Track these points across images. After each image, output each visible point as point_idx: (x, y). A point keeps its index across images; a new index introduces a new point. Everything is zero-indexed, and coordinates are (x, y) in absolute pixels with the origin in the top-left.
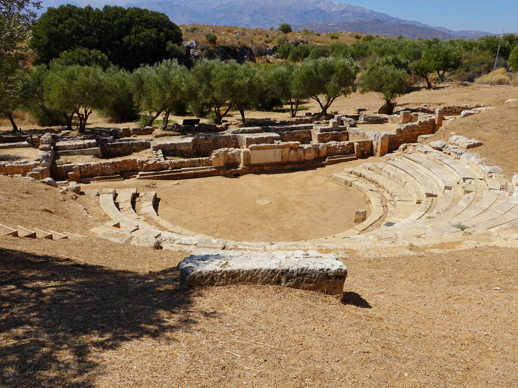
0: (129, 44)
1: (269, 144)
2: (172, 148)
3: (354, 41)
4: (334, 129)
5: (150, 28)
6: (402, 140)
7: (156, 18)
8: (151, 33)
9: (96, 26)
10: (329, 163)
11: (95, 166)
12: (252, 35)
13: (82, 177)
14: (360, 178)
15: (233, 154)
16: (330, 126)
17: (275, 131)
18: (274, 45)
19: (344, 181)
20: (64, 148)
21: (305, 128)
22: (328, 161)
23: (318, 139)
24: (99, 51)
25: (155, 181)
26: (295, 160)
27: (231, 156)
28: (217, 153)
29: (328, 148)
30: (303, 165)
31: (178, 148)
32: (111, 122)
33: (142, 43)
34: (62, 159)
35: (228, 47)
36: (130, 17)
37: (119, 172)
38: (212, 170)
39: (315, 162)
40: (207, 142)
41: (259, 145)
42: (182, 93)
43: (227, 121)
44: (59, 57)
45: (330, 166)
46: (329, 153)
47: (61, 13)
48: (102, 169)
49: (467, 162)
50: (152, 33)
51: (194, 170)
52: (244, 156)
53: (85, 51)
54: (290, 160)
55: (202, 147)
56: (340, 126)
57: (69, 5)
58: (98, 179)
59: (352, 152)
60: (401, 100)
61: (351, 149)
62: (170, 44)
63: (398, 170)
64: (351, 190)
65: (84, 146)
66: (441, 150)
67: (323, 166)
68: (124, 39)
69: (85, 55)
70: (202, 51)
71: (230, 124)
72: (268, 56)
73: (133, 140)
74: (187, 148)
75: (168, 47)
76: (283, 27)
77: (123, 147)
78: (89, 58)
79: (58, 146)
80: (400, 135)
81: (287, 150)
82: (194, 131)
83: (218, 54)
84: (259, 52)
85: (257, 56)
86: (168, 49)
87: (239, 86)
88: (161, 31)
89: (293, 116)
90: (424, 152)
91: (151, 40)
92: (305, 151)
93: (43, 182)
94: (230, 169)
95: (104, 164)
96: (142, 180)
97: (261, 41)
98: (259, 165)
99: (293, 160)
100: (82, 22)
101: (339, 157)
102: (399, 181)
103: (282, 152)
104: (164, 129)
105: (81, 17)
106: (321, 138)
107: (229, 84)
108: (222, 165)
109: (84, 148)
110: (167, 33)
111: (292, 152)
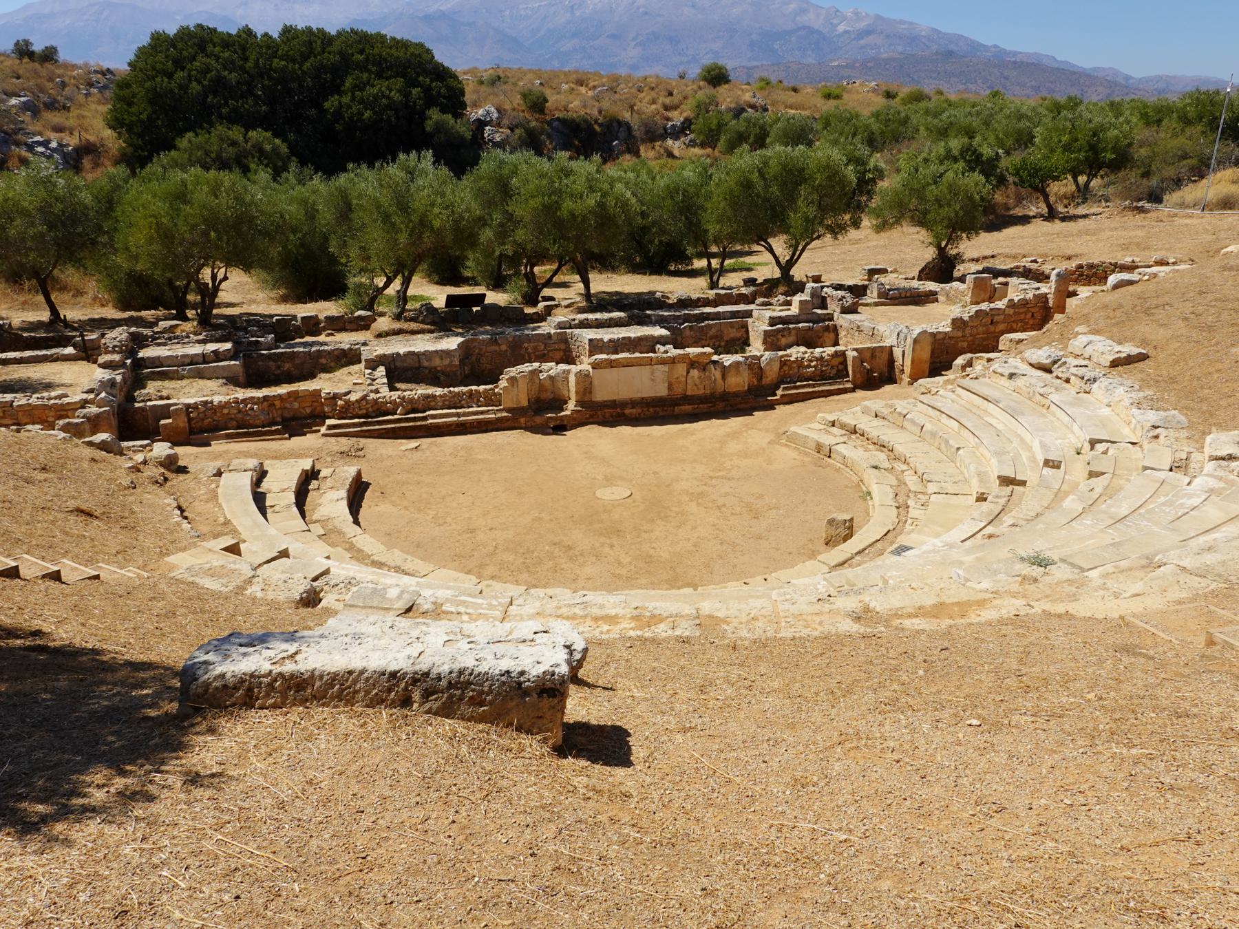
0: (338, 115)
1: (637, 355)
2: (410, 362)
3: (880, 102)
4: (803, 317)
5: (387, 79)
6: (965, 344)
7: (401, 54)
8: (391, 91)
9: (261, 75)
10: (786, 400)
11: (222, 406)
12: (634, 91)
13: (192, 431)
14: (853, 436)
15: (551, 378)
16: (794, 310)
17: (661, 322)
18: (685, 114)
19: (813, 445)
20: (156, 362)
21: (734, 314)
22: (782, 396)
23: (765, 342)
24: (268, 134)
25: (363, 441)
26: (702, 392)
27: (548, 383)
28: (512, 374)
29: (784, 363)
30: (720, 406)
31: (426, 364)
32: (284, 299)
33: (367, 114)
34: (152, 387)
35: (573, 120)
36: (340, 53)
37: (279, 419)
38: (499, 415)
39: (753, 397)
40: (497, 348)
41: (614, 357)
42: (438, 233)
43: (552, 299)
44: (175, 147)
45: (788, 407)
46: (785, 376)
47: (180, 45)
48: (240, 411)
49: (1106, 401)
50: (393, 89)
51: (458, 415)
52: (577, 383)
53: (236, 133)
54: (689, 393)
55: (484, 360)
56: (819, 311)
57: (200, 26)
58: (228, 436)
59: (842, 373)
60: (976, 248)
61: (841, 367)
62: (434, 115)
63: (944, 419)
64: (829, 465)
65: (204, 358)
66: (1048, 370)
67: (771, 406)
68: (327, 105)
69: (234, 143)
70: (512, 130)
71: (557, 306)
72: (670, 142)
73: (322, 344)
74: (446, 362)
75: (430, 122)
76: (709, 72)
77: (297, 361)
78: (245, 150)
79: (142, 359)
80: (960, 334)
81: (681, 369)
82: (469, 322)
83: (549, 136)
84: (647, 132)
85: (643, 141)
86: (429, 126)
87: (573, 216)
88: (415, 84)
89: (713, 285)
90: (1006, 374)
91: (388, 107)
92: (725, 371)
93: (91, 444)
94: (542, 414)
95: (244, 401)
96: (333, 439)
97: (654, 107)
98: (613, 404)
99: (697, 393)
100: (230, 65)
101: (809, 386)
102: (943, 446)
104: (398, 317)
105: (227, 54)
106: (771, 341)
107: (550, 210)
108: (525, 403)
109: (205, 362)
110: (427, 90)
111: (695, 373)
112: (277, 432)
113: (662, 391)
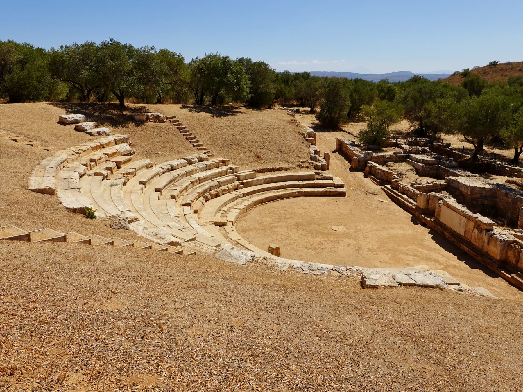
2: (456, 185)
10: (513, 281)
26: (477, 245)
30: (479, 258)
31: (460, 189)
40: (507, 199)
51: (406, 200)
55: (501, 203)
58: (372, 178)
74: (466, 191)
81: (471, 225)
98: (444, 227)
99: (474, 243)
103: (467, 224)
111: (476, 231)
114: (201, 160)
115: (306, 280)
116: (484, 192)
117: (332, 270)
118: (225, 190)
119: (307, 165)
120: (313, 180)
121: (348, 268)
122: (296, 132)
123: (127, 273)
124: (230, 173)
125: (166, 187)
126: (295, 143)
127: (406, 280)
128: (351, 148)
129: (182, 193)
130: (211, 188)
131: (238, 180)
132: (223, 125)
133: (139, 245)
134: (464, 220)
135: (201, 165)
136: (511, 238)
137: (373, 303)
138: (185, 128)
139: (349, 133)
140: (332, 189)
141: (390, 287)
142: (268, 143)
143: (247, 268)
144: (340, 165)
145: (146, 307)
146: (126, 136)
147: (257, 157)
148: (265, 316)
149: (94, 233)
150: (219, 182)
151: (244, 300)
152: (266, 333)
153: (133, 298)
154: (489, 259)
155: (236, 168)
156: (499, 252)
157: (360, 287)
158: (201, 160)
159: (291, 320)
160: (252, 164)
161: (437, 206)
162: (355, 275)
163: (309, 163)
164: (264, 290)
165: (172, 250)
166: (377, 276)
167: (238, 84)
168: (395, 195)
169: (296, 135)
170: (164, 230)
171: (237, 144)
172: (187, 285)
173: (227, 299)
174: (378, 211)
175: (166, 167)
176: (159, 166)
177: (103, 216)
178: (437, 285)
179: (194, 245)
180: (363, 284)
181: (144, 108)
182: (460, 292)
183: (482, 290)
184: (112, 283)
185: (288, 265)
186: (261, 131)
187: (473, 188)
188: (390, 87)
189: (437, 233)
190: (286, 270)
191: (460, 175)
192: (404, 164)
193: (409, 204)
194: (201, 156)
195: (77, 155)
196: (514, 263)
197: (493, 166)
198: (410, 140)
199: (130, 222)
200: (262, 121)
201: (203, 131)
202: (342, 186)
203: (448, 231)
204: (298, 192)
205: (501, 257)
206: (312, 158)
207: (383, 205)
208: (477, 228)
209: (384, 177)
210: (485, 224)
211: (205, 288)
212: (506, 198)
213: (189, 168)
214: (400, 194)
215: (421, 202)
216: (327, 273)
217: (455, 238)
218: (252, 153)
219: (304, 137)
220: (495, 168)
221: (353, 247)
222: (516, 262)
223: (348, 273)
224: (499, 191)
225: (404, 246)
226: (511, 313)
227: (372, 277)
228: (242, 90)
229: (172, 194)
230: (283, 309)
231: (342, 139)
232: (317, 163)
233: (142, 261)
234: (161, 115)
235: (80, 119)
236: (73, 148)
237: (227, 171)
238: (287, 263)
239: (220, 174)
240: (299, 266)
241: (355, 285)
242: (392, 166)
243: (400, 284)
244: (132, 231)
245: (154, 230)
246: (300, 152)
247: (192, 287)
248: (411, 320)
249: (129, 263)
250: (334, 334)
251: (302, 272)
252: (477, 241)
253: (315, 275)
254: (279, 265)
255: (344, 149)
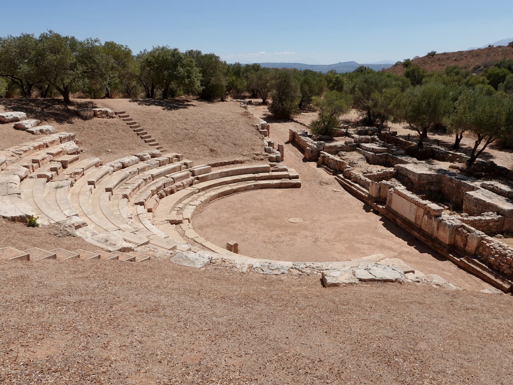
2: (404, 173)
10: (462, 265)
26: (427, 230)
31: (409, 176)
51: (358, 189)
55: (446, 188)
58: (325, 168)
74: (414, 178)
81: (421, 211)
98: (395, 214)
103: (417, 210)
111: (426, 217)
112: (331, 172)
113: (412, 218)
114: (153, 156)
115: (266, 281)
116: (430, 178)
117: (292, 268)
118: (180, 186)
119: (262, 157)
120: (268, 172)
121: (308, 265)
122: (249, 125)
123: (68, 298)
124: (184, 168)
125: (117, 186)
126: (249, 135)
127: (366, 276)
128: (303, 138)
129: (135, 191)
130: (164, 185)
131: (193, 175)
132: (175, 119)
133: (87, 255)
134: (414, 207)
135: (154, 161)
136: (458, 223)
137: (337, 311)
138: (135, 123)
139: (301, 124)
140: (288, 181)
141: (351, 284)
142: (222, 136)
143: (204, 272)
144: (294, 156)
145: (85, 348)
146: (72, 134)
147: (212, 150)
148: (225, 346)
149: (34, 245)
150: (173, 178)
151: (200, 323)
152: (227, 372)
153: (70, 337)
154: (439, 244)
155: (190, 163)
156: (448, 237)
157: (321, 286)
158: (153, 156)
159: (253, 348)
160: (207, 158)
161: (388, 194)
162: (315, 272)
163: (264, 155)
164: (223, 305)
165: (124, 257)
166: (339, 273)
167: (189, 77)
168: (348, 184)
169: (250, 127)
170: (115, 236)
171: (191, 138)
172: (136, 309)
173: (182, 324)
174: (333, 201)
175: (117, 165)
176: (109, 164)
177: (46, 223)
178: (397, 279)
179: (148, 249)
180: (323, 281)
181: (92, 103)
182: (418, 284)
183: (437, 279)
184: (47, 314)
185: (247, 266)
186: (214, 124)
187: (420, 175)
188: (338, 77)
189: (390, 220)
190: (245, 272)
191: (407, 163)
192: (355, 153)
193: (361, 193)
194: (154, 152)
195: (18, 156)
196: (462, 246)
197: (437, 152)
198: (359, 129)
199: (78, 227)
200: (215, 114)
201: (155, 125)
202: (297, 177)
203: (399, 218)
204: (254, 185)
205: (450, 242)
206: (266, 150)
207: (338, 195)
208: (427, 214)
209: (337, 167)
210: (434, 210)
211: (156, 310)
212: (450, 183)
213: (142, 165)
214: (352, 183)
215: (373, 191)
216: (287, 272)
217: (406, 225)
218: (206, 148)
219: (258, 129)
220: (439, 154)
221: (310, 238)
222: (464, 246)
223: (308, 271)
224: (444, 177)
225: (360, 235)
226: (473, 309)
227: (332, 274)
228: (193, 83)
229: (124, 193)
230: (244, 331)
231: (295, 130)
232: (272, 155)
233: (87, 278)
234: (110, 111)
235: (19, 117)
236: (12, 149)
237: (181, 167)
238: (246, 263)
239: (174, 170)
240: (258, 266)
241: (315, 284)
242: (343, 156)
243: (360, 280)
244: (80, 238)
245: (103, 235)
246: (254, 145)
247: (143, 311)
248: (380, 331)
249: (72, 282)
250: (301, 363)
251: (262, 272)
252: (427, 227)
253: (275, 275)
254: (238, 267)
255: (296, 140)
